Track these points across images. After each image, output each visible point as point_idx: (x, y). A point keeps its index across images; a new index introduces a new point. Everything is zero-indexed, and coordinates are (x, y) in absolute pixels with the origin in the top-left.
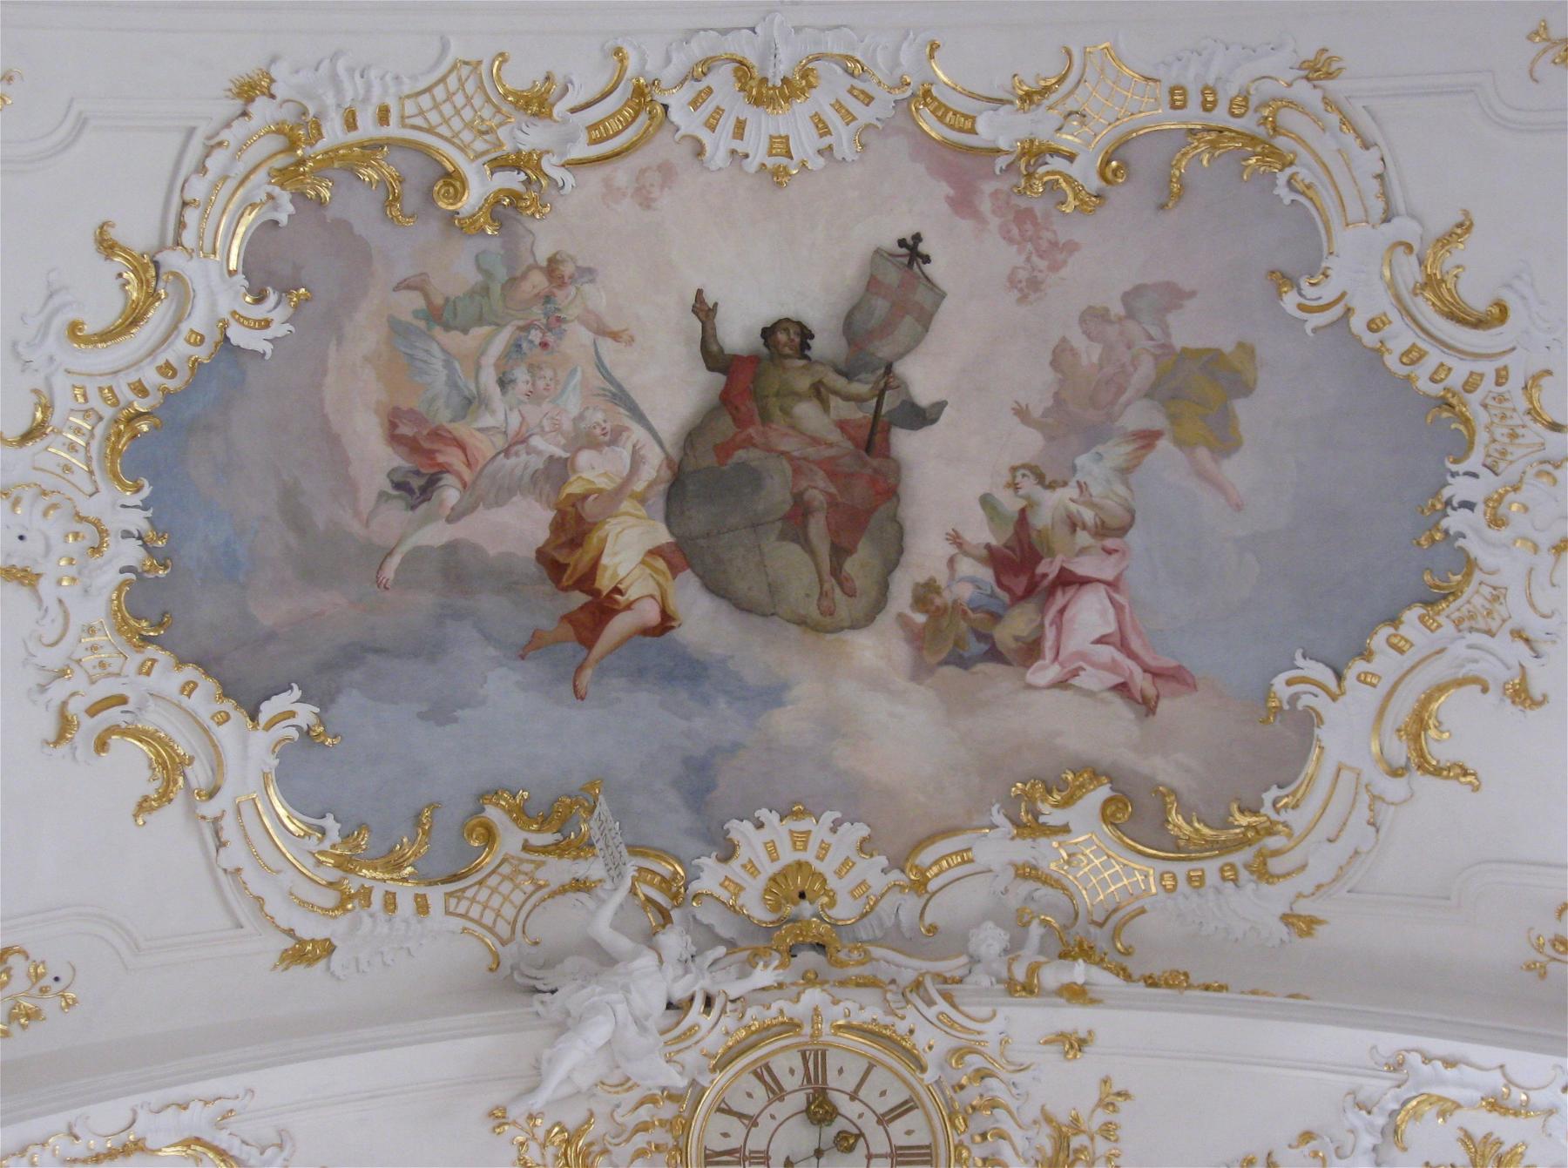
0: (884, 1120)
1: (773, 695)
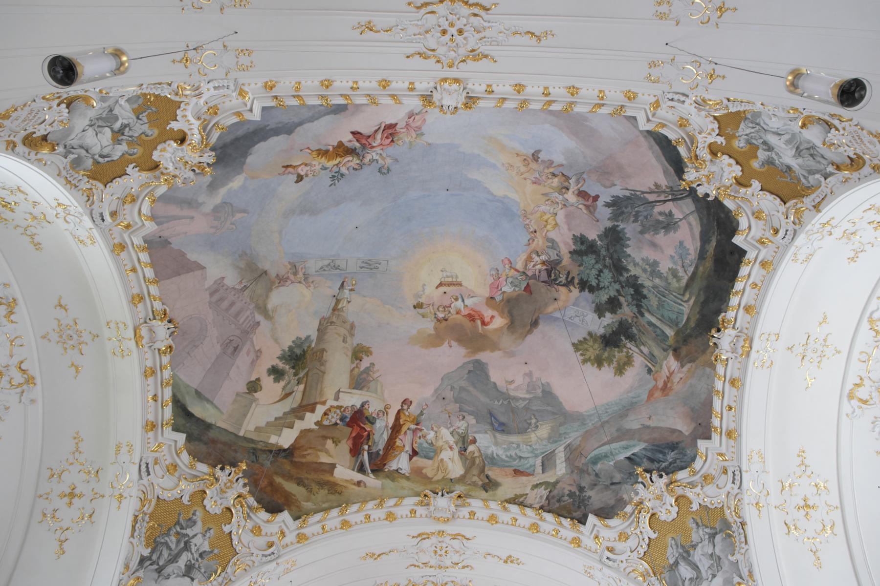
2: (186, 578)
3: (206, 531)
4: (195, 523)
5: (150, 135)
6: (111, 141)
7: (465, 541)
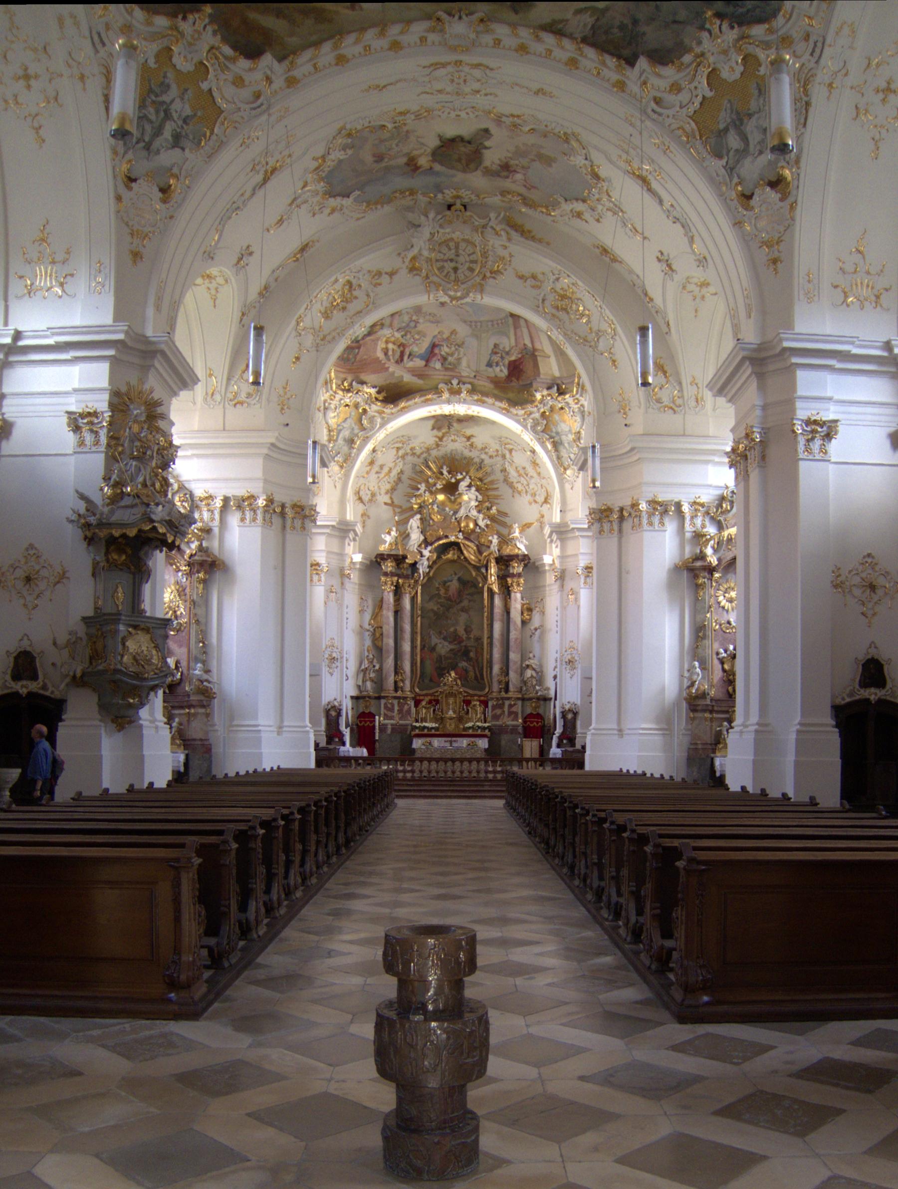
0: (469, 255)
1: (453, 176)
2: (176, 149)
3: (183, 94)
4: (168, 86)
7: (488, 71)
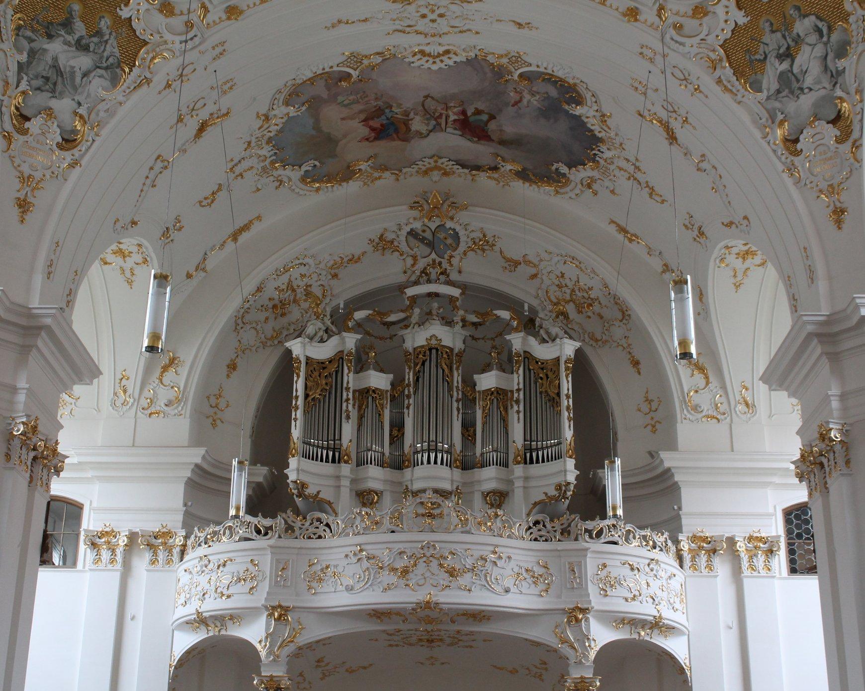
5: (769, 23)
6: (802, 48)
